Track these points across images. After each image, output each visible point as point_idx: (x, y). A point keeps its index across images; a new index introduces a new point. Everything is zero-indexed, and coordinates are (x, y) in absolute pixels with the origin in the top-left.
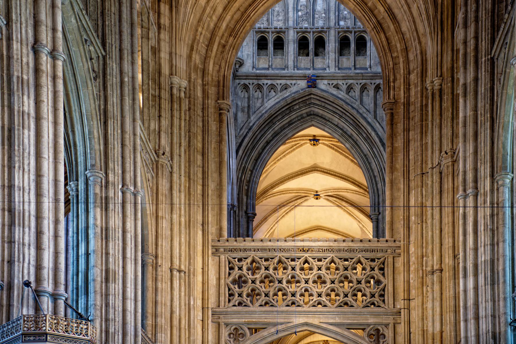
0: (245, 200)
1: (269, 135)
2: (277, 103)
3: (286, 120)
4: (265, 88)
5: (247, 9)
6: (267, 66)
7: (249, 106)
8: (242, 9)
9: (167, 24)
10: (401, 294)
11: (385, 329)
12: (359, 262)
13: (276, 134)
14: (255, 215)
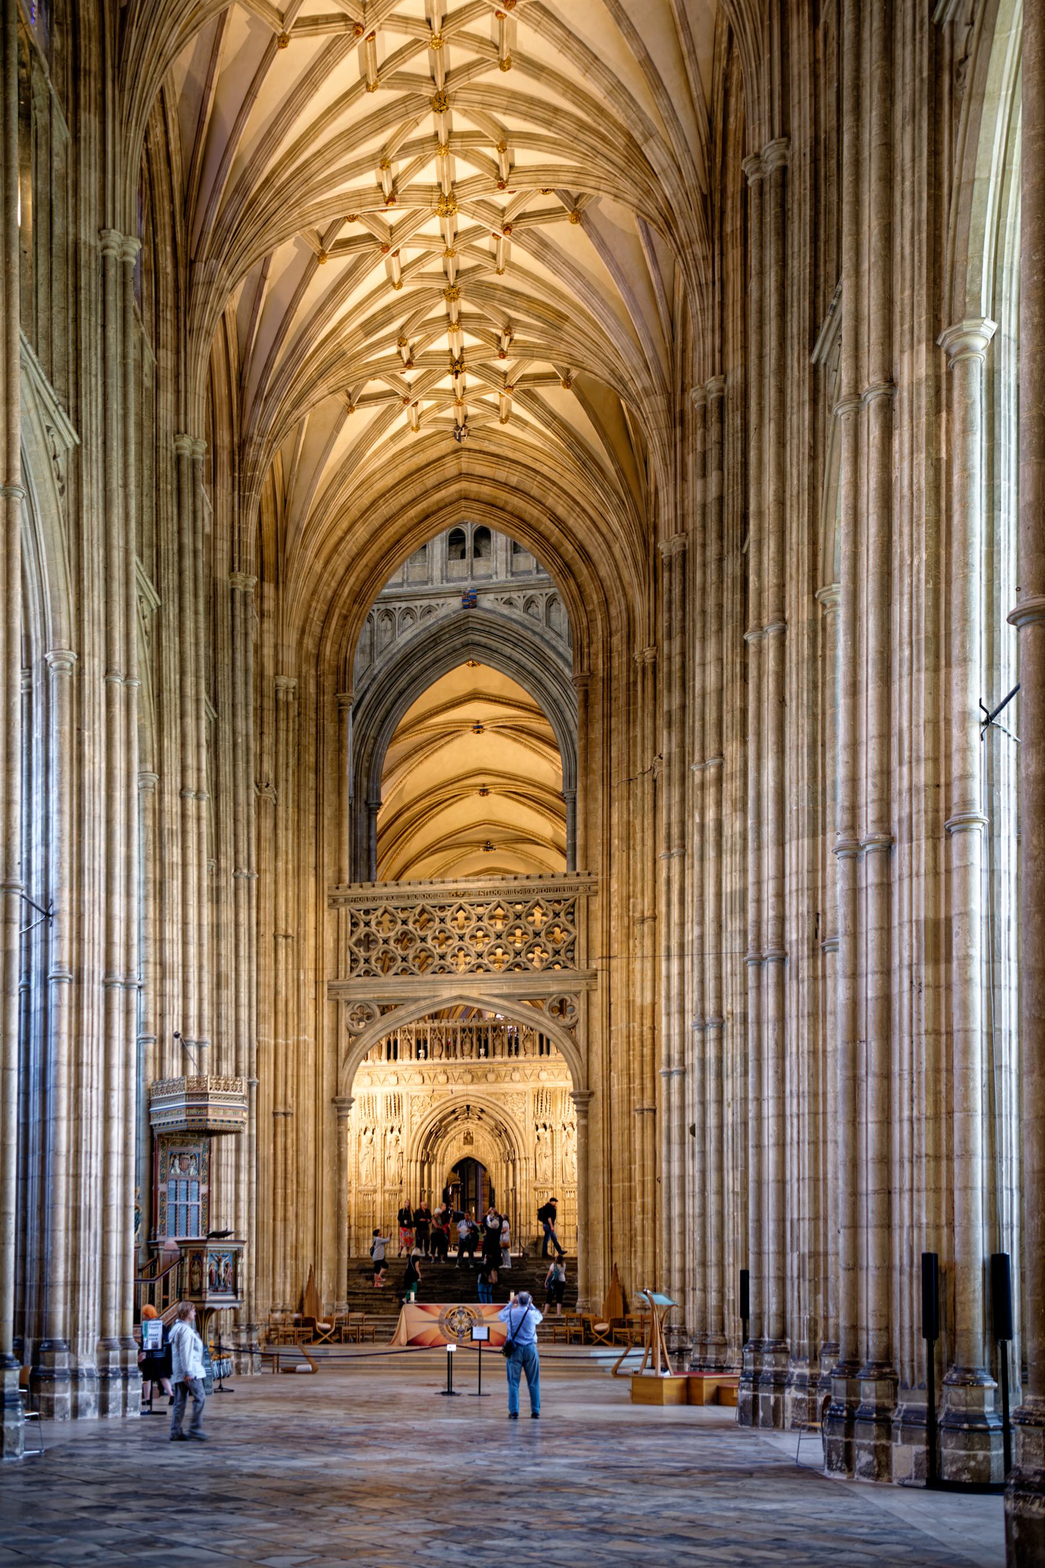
0: (365, 783)
1: (402, 683)
2: (416, 636)
3: (430, 657)
4: (397, 614)
5: (377, 565)
6: (400, 580)
7: (372, 644)
8: (371, 565)
9: (272, 609)
10: (598, 951)
11: (575, 999)
12: (538, 904)
13: (414, 680)
14: (381, 804)
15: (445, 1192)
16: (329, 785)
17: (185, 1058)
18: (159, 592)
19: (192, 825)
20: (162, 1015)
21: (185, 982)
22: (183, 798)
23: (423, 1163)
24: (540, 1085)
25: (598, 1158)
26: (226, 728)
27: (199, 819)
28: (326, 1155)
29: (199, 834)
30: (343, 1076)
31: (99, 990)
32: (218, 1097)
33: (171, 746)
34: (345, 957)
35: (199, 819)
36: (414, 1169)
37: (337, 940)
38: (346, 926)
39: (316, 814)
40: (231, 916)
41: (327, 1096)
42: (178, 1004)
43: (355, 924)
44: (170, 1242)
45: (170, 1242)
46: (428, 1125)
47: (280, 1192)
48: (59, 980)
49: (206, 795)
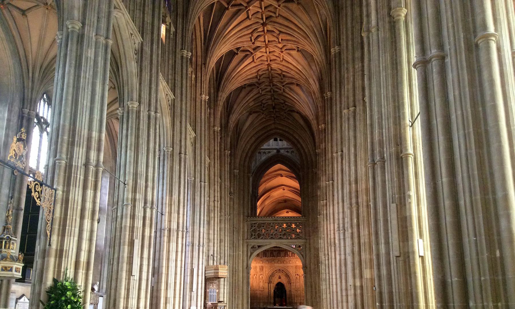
15: (274, 291)
16: (246, 194)
17: (214, 260)
18: (210, 159)
19: (216, 208)
20: (209, 251)
21: (214, 243)
22: (214, 203)
23: (269, 283)
24: (296, 265)
25: (308, 284)
26: (223, 184)
27: (218, 207)
28: (245, 281)
29: (218, 210)
30: (249, 262)
31: (197, 247)
32: (221, 270)
33: (212, 192)
34: (250, 234)
35: (218, 207)
36: (266, 285)
37: (248, 230)
38: (250, 227)
39: (243, 201)
40: (224, 226)
41: (245, 267)
42: (212, 248)
43: (252, 226)
44: (209, 303)
45: (209, 303)
46: (270, 274)
47: (234, 290)
48: (189, 246)
49: (219, 202)
